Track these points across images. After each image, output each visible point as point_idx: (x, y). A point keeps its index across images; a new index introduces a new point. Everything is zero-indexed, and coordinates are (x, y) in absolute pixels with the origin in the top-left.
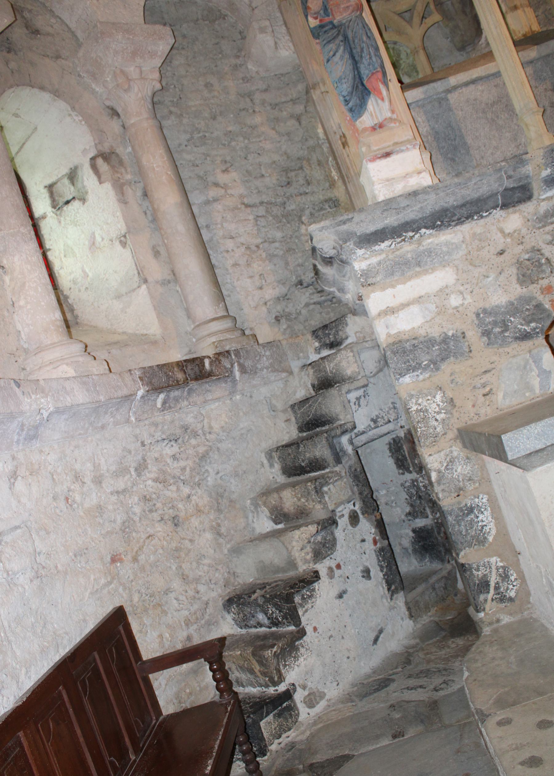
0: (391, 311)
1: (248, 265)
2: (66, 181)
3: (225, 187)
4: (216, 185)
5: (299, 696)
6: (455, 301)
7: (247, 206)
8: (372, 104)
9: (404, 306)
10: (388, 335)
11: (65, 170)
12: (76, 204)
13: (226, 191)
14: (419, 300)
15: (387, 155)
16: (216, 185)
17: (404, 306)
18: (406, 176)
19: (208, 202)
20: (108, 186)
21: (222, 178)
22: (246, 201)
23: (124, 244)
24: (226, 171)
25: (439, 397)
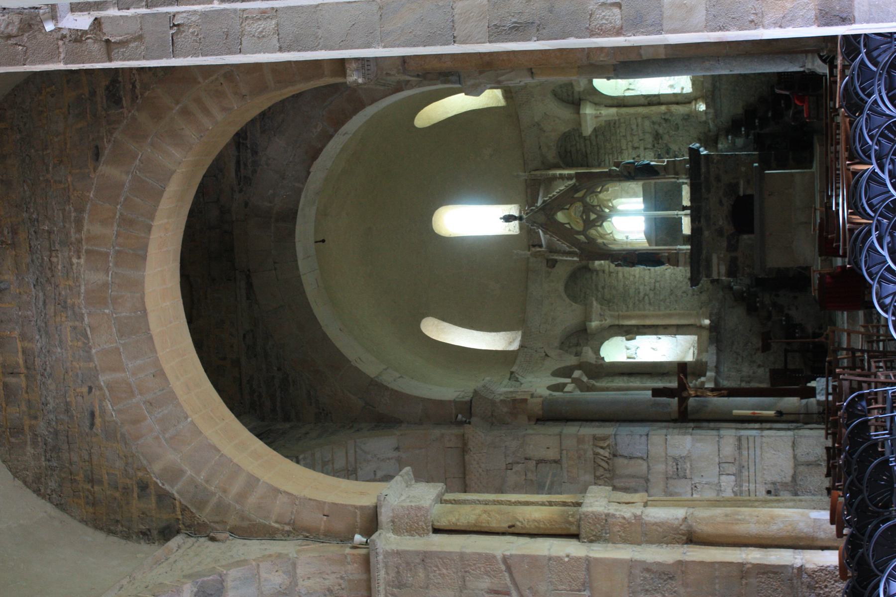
0: (719, 273)
1: (677, 296)
2: (628, 351)
3: (645, 295)
4: (644, 298)
5: (817, 331)
6: (722, 256)
7: (654, 289)
8: (663, 260)
9: (719, 270)
10: (725, 276)
11: (625, 350)
12: (638, 351)
13: (647, 295)
14: (718, 265)
15: (678, 261)
16: (644, 298)
17: (719, 270)
18: (685, 257)
19: (650, 304)
20: (638, 337)
21: (642, 295)
22: (652, 289)
23: (660, 338)
24: (639, 293)
25: (746, 269)
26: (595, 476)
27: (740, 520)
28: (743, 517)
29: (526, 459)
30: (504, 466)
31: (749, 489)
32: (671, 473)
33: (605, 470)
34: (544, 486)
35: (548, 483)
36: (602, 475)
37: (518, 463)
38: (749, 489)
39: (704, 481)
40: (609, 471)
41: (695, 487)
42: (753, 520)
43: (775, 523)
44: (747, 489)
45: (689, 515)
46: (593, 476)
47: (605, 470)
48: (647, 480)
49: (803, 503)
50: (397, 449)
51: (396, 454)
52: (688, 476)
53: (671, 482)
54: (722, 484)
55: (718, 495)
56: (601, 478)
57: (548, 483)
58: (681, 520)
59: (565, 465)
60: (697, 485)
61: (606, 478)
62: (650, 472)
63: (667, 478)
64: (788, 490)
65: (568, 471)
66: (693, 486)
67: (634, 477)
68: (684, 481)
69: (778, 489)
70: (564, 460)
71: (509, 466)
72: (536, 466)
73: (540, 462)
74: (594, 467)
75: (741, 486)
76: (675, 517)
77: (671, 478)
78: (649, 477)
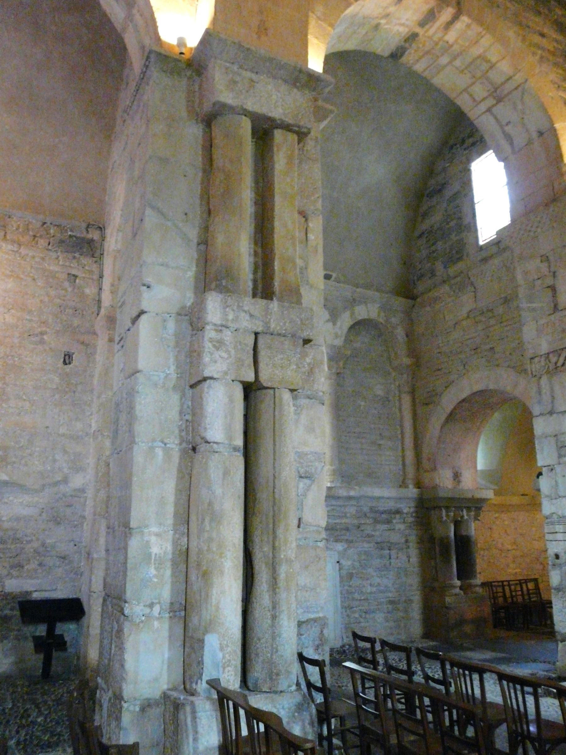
26: (548, 354)
27: (202, 523)
28: (208, 528)
29: (554, 273)
30: (543, 252)
31: (556, 533)
32: (562, 439)
33: (556, 363)
34: (531, 302)
35: (534, 305)
36: (550, 362)
37: (549, 267)
38: (556, 533)
39: (560, 480)
40: (556, 368)
41: (552, 469)
42: (202, 544)
43: (198, 579)
44: (557, 530)
45: (212, 447)
46: (547, 352)
47: (556, 363)
48: (551, 413)
49: (269, 622)
50: (541, 134)
51: (535, 135)
52: (561, 461)
53: (553, 440)
54: (558, 500)
55: (547, 496)
56: (547, 360)
57: (534, 305)
58: (203, 435)
59: (552, 317)
60: (554, 471)
61: (549, 367)
62: (560, 415)
63: (555, 436)
64: (562, 580)
65: (548, 323)
66: (552, 467)
67: (553, 397)
68: (556, 455)
69: (561, 568)
70: (558, 314)
71: (545, 259)
72: (549, 287)
73: (553, 289)
74: (556, 351)
75: (559, 523)
76: (208, 426)
77: (557, 440)
78: (555, 415)
